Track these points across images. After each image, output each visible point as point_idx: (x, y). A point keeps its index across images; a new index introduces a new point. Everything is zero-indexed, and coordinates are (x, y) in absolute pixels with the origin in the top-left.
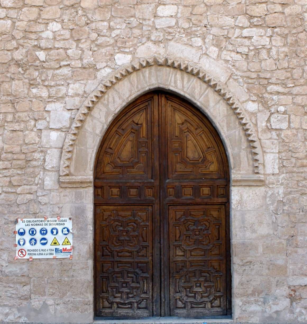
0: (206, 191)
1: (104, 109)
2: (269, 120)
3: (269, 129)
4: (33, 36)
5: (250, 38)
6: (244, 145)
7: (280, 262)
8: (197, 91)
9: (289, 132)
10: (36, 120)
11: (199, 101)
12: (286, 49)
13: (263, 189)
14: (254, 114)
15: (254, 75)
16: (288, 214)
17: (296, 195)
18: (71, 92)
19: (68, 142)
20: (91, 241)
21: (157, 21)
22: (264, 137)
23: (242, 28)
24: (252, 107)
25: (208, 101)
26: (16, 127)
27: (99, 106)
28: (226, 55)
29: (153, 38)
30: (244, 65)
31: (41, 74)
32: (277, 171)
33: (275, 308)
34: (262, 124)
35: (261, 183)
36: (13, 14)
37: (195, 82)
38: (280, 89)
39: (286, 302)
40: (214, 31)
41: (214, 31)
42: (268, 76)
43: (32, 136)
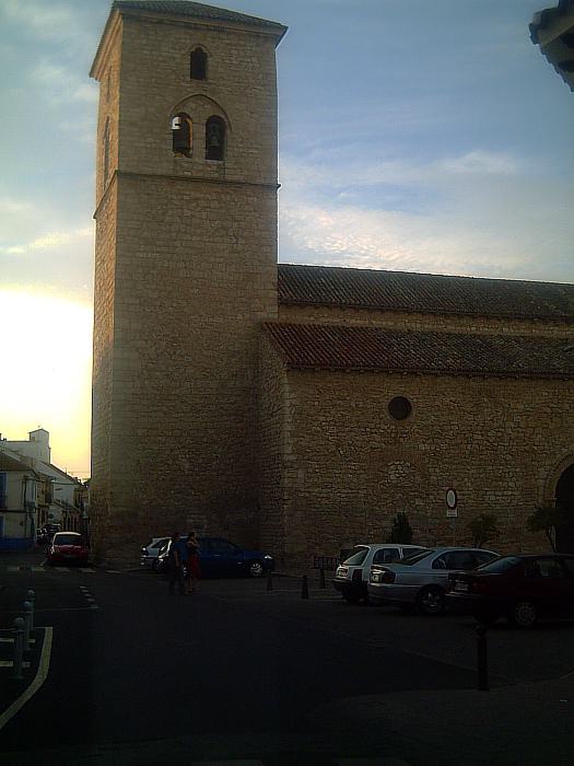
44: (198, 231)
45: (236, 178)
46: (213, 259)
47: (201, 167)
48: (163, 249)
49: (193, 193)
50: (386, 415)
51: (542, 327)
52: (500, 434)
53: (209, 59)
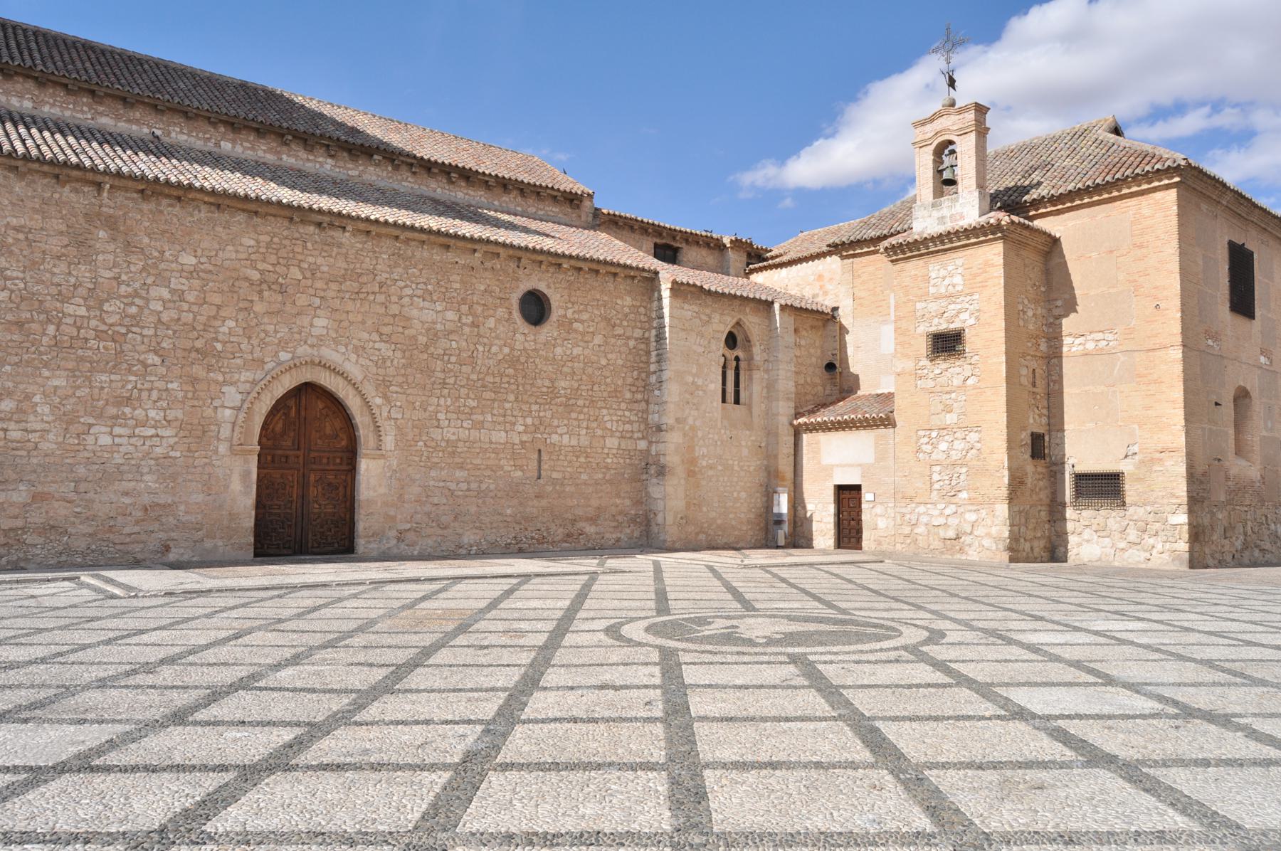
0: (338, 461)
1: (269, 395)
3: (390, 418)
4: (211, 329)
5: (379, 350)
7: (392, 513)
8: (340, 386)
10: (212, 399)
12: (403, 361)
13: (383, 461)
14: (379, 407)
15: (381, 378)
16: (399, 480)
17: (405, 466)
18: (243, 379)
20: (254, 497)
21: (313, 329)
23: (375, 342)
24: (379, 401)
26: (196, 403)
28: (362, 361)
29: (309, 342)
30: (374, 370)
31: (217, 361)
33: (387, 546)
34: (385, 414)
35: (383, 456)
36: (195, 308)
37: (340, 380)
39: (395, 542)
40: (354, 341)
41: (354, 341)
43: (208, 412)
51: (303, 154)
52: (133, 310)
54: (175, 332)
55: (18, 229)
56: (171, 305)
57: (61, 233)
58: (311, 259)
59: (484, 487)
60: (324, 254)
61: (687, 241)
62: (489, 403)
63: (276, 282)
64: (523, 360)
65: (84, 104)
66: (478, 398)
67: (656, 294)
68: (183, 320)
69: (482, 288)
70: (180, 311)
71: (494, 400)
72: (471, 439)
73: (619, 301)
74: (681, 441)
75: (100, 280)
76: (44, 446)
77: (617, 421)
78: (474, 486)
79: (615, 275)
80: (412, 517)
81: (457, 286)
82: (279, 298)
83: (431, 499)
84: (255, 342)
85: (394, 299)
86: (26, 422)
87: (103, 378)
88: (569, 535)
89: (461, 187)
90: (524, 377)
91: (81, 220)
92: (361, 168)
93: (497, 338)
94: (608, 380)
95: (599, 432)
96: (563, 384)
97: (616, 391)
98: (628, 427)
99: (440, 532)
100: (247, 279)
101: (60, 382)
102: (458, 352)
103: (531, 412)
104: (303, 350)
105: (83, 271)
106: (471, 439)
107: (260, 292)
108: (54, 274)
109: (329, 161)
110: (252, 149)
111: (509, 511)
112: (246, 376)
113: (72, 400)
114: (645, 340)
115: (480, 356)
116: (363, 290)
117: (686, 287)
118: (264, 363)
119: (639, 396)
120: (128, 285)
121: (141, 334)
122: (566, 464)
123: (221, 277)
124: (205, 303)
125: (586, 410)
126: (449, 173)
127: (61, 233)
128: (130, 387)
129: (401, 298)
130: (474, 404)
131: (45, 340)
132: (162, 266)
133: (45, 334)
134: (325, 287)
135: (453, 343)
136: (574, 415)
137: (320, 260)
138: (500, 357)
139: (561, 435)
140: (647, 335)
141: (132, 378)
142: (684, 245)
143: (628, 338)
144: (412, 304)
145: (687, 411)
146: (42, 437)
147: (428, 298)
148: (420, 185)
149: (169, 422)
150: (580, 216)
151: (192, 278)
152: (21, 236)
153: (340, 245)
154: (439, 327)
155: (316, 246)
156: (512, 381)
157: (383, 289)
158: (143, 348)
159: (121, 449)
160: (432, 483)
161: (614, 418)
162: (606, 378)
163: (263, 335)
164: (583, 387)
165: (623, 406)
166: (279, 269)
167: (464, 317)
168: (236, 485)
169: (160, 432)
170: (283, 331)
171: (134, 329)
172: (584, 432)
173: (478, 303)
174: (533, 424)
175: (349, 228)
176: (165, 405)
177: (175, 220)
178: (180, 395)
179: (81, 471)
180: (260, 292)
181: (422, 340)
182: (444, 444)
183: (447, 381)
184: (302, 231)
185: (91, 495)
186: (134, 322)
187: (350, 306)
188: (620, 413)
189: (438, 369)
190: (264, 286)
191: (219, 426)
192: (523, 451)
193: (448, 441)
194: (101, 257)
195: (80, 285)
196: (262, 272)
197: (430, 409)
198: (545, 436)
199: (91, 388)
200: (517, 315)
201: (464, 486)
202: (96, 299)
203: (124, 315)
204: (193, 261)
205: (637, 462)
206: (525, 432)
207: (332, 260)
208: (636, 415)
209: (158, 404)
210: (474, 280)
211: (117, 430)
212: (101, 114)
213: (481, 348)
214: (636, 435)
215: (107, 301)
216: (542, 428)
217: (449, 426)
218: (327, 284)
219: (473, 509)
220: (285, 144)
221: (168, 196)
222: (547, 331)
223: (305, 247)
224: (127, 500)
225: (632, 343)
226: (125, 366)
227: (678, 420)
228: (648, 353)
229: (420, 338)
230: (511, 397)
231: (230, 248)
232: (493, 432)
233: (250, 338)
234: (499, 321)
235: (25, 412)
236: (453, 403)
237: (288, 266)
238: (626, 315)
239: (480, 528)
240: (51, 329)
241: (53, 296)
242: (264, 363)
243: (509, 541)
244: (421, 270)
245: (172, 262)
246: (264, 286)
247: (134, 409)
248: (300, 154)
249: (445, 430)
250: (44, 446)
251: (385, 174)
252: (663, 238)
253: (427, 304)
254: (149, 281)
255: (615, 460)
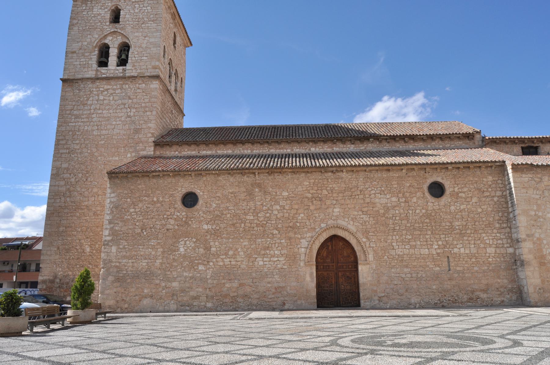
0: (350, 267)
1: (318, 241)
2: (370, 244)
3: (370, 247)
4: (295, 218)
5: (363, 218)
6: (362, 252)
7: (375, 289)
8: (347, 235)
9: (376, 248)
11: (348, 239)
12: (374, 222)
13: (368, 266)
14: (365, 242)
15: (364, 230)
17: (379, 267)
19: (308, 252)
22: (368, 249)
23: (360, 215)
24: (364, 240)
25: (350, 238)
26: (291, 247)
27: (317, 240)
28: (356, 224)
30: (361, 227)
31: (298, 230)
32: (373, 260)
33: (374, 303)
34: (368, 245)
35: (368, 264)
36: (289, 211)
38: (373, 234)
39: (377, 302)
40: (352, 216)
42: (369, 230)
43: (296, 250)
44: (107, 107)
45: (132, 74)
46: (114, 123)
47: (112, 72)
48: (85, 120)
49: (105, 86)
50: (179, 205)
51: (341, 146)
52: (268, 215)
53: (121, 11)
54: (282, 221)
55: (232, 193)
56: (281, 211)
57: (244, 192)
58: (331, 186)
59: (419, 275)
60: (336, 183)
61: (542, 142)
62: (418, 236)
63: (318, 197)
64: (433, 214)
65: (266, 147)
66: (412, 235)
67: (506, 172)
68: (285, 216)
69: (408, 185)
70: (284, 213)
71: (420, 235)
72: (410, 253)
73: (484, 179)
74: (532, 246)
75: (257, 206)
76: (242, 266)
77: (493, 239)
78: (414, 275)
79: (480, 167)
80: (384, 290)
81: (396, 186)
82: (319, 203)
83: (393, 282)
84: (311, 221)
85: (367, 196)
86: (236, 258)
87: (259, 241)
88: (471, 299)
89: (411, 143)
90: (435, 222)
91: (250, 186)
92: (365, 146)
93: (418, 206)
94: (484, 219)
95: (482, 246)
96: (457, 223)
97: (489, 224)
98: (499, 242)
99: (399, 297)
100: (307, 197)
101: (246, 243)
102: (399, 215)
103: (441, 238)
104: (330, 222)
105: (251, 204)
106: (410, 253)
107: (312, 202)
108: (243, 206)
109: (352, 146)
110: (323, 148)
111: (434, 287)
112: (309, 235)
113: (250, 249)
114: (505, 197)
115: (410, 215)
116: (353, 194)
117: (521, 166)
118: (315, 229)
119: (505, 225)
120: (266, 206)
121: (271, 223)
122: (464, 262)
123: (297, 198)
124: (292, 209)
125: (472, 235)
126: (404, 139)
127: (244, 192)
128: (268, 243)
129: (370, 195)
130: (411, 237)
131: (241, 229)
132: (277, 198)
133: (241, 227)
134: (337, 196)
135: (397, 211)
136: (465, 238)
137: (334, 185)
138: (421, 214)
139: (459, 248)
140: (504, 193)
141: (269, 240)
142: (540, 144)
143: (493, 197)
144: (375, 197)
145: (534, 230)
146: (241, 263)
147: (383, 193)
148: (392, 146)
149: (282, 255)
150: (474, 143)
151: (287, 200)
152: (233, 195)
153: (342, 178)
154: (389, 205)
155: (332, 180)
156: (429, 225)
157: (362, 193)
158: (271, 228)
159: (267, 266)
160: (393, 275)
161: (490, 238)
162: (482, 218)
163: (314, 218)
164: (469, 224)
165: (495, 231)
166: (319, 192)
167: (400, 199)
168: (308, 279)
169: (280, 259)
170: (322, 216)
171: (269, 222)
172: (473, 246)
173: (407, 192)
174: (443, 244)
175: (344, 171)
176: (280, 249)
177: (280, 180)
178: (285, 244)
179: (254, 275)
180: (312, 202)
181: (382, 211)
182: (397, 257)
183: (396, 228)
184: (326, 175)
185: (257, 284)
186: (268, 219)
187: (348, 202)
188: (494, 235)
189: (391, 223)
190: (314, 199)
191: (300, 255)
192: (439, 257)
193: (399, 255)
194: (257, 198)
195: (251, 209)
196: (312, 194)
197: (389, 241)
198: (450, 249)
199: (256, 244)
200: (427, 194)
201: (409, 275)
202: (256, 213)
203: (265, 217)
204: (287, 194)
205: (508, 260)
206: (439, 248)
207: (339, 185)
208: (504, 235)
209: (278, 248)
210: (404, 182)
211: (265, 259)
212: (271, 149)
213: (411, 212)
214: (505, 246)
215: (259, 213)
216: (448, 246)
217: (398, 248)
218: (338, 194)
219: (415, 286)
220: (335, 143)
221: (277, 172)
222: (444, 200)
223: (328, 181)
224: (269, 285)
225: (496, 199)
226: (266, 235)
227: (528, 235)
228: (507, 203)
229: (380, 211)
230: (429, 233)
231: (300, 187)
232: (421, 250)
233: (309, 220)
234: (418, 198)
235: (236, 255)
236: (399, 238)
237: (322, 190)
238: (490, 186)
239: (420, 296)
240: (243, 225)
241: (243, 214)
242: (315, 229)
243: (436, 302)
244: (378, 182)
245: (280, 195)
246: (314, 199)
247: (270, 251)
248: (340, 146)
249: (397, 250)
250: (242, 266)
251: (376, 146)
252: (526, 144)
253: (382, 196)
254: (273, 204)
255: (494, 259)
